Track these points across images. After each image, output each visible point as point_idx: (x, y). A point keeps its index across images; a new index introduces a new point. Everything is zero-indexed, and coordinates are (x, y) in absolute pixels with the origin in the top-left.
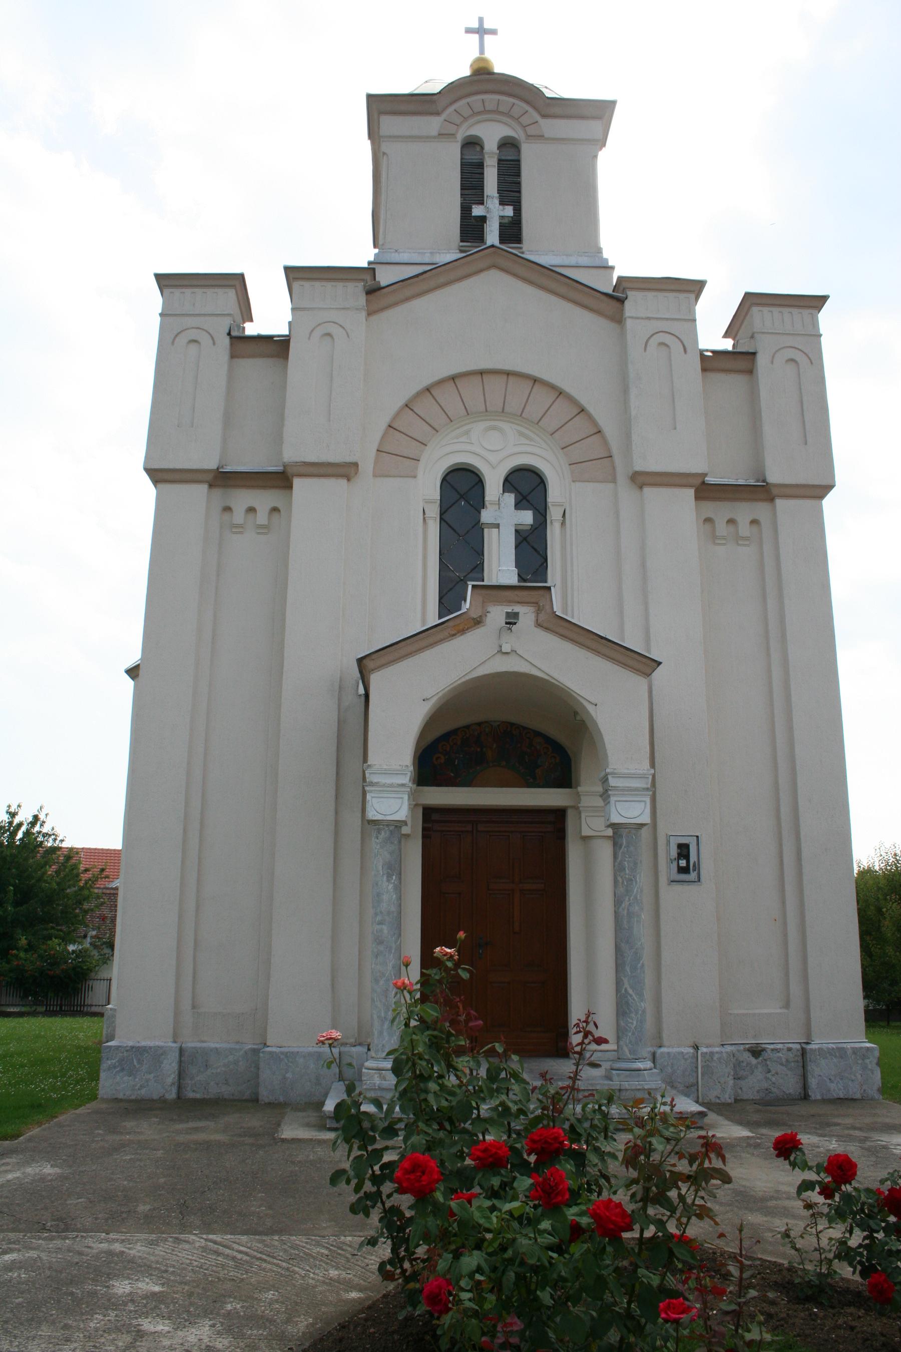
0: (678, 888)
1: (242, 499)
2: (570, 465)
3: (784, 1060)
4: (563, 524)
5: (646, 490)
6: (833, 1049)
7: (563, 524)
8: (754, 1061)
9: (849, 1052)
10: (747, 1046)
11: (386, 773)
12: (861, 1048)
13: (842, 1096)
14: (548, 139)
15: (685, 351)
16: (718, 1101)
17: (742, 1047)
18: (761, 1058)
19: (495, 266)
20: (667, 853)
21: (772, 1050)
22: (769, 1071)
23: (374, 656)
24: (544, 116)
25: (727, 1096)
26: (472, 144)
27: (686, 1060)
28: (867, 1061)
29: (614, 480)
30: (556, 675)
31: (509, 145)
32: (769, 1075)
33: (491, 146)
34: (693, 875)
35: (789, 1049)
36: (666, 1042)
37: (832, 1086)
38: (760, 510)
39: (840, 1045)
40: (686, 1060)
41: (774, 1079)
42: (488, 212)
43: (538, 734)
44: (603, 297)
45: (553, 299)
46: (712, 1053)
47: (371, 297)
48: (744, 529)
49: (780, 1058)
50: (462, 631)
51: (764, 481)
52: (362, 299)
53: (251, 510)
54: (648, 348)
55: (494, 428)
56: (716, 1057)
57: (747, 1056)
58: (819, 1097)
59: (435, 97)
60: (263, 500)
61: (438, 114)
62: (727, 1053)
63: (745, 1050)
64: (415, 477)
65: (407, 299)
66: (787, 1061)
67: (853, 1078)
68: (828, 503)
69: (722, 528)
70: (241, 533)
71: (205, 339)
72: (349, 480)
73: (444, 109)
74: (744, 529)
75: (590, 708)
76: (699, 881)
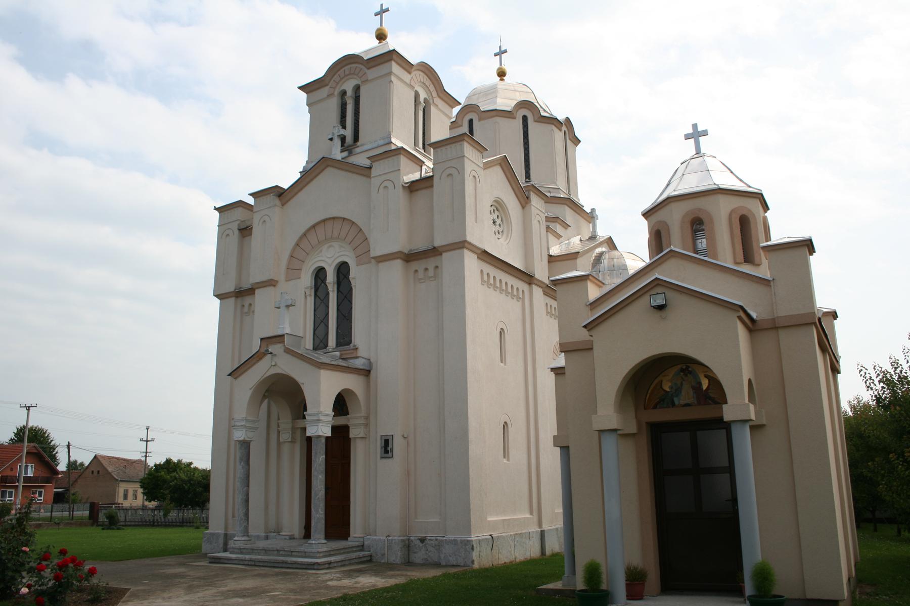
0: (384, 461)
3: (434, 545)
5: (381, 264)
6: (452, 540)
8: (421, 545)
9: (459, 542)
10: (420, 537)
11: (239, 421)
12: (464, 540)
13: (455, 564)
14: (370, 80)
15: (395, 188)
16: (394, 563)
17: (417, 538)
18: (424, 543)
19: (328, 166)
20: (379, 444)
21: (429, 539)
22: (427, 550)
23: (233, 374)
25: (398, 560)
27: (381, 542)
28: (467, 547)
32: (427, 552)
34: (390, 454)
35: (436, 540)
36: (378, 534)
37: (451, 558)
39: (456, 538)
40: (381, 542)
41: (429, 554)
44: (366, 169)
45: (350, 174)
46: (392, 540)
47: (281, 198)
48: (431, 272)
49: (432, 543)
50: (261, 359)
52: (277, 201)
55: (330, 246)
56: (394, 541)
57: (418, 542)
58: (444, 564)
59: (323, 79)
61: (327, 85)
62: (398, 540)
63: (418, 539)
64: (300, 278)
65: (297, 193)
66: (435, 545)
67: (460, 555)
69: (421, 274)
70: (248, 315)
72: (274, 286)
73: (329, 82)
76: (392, 457)
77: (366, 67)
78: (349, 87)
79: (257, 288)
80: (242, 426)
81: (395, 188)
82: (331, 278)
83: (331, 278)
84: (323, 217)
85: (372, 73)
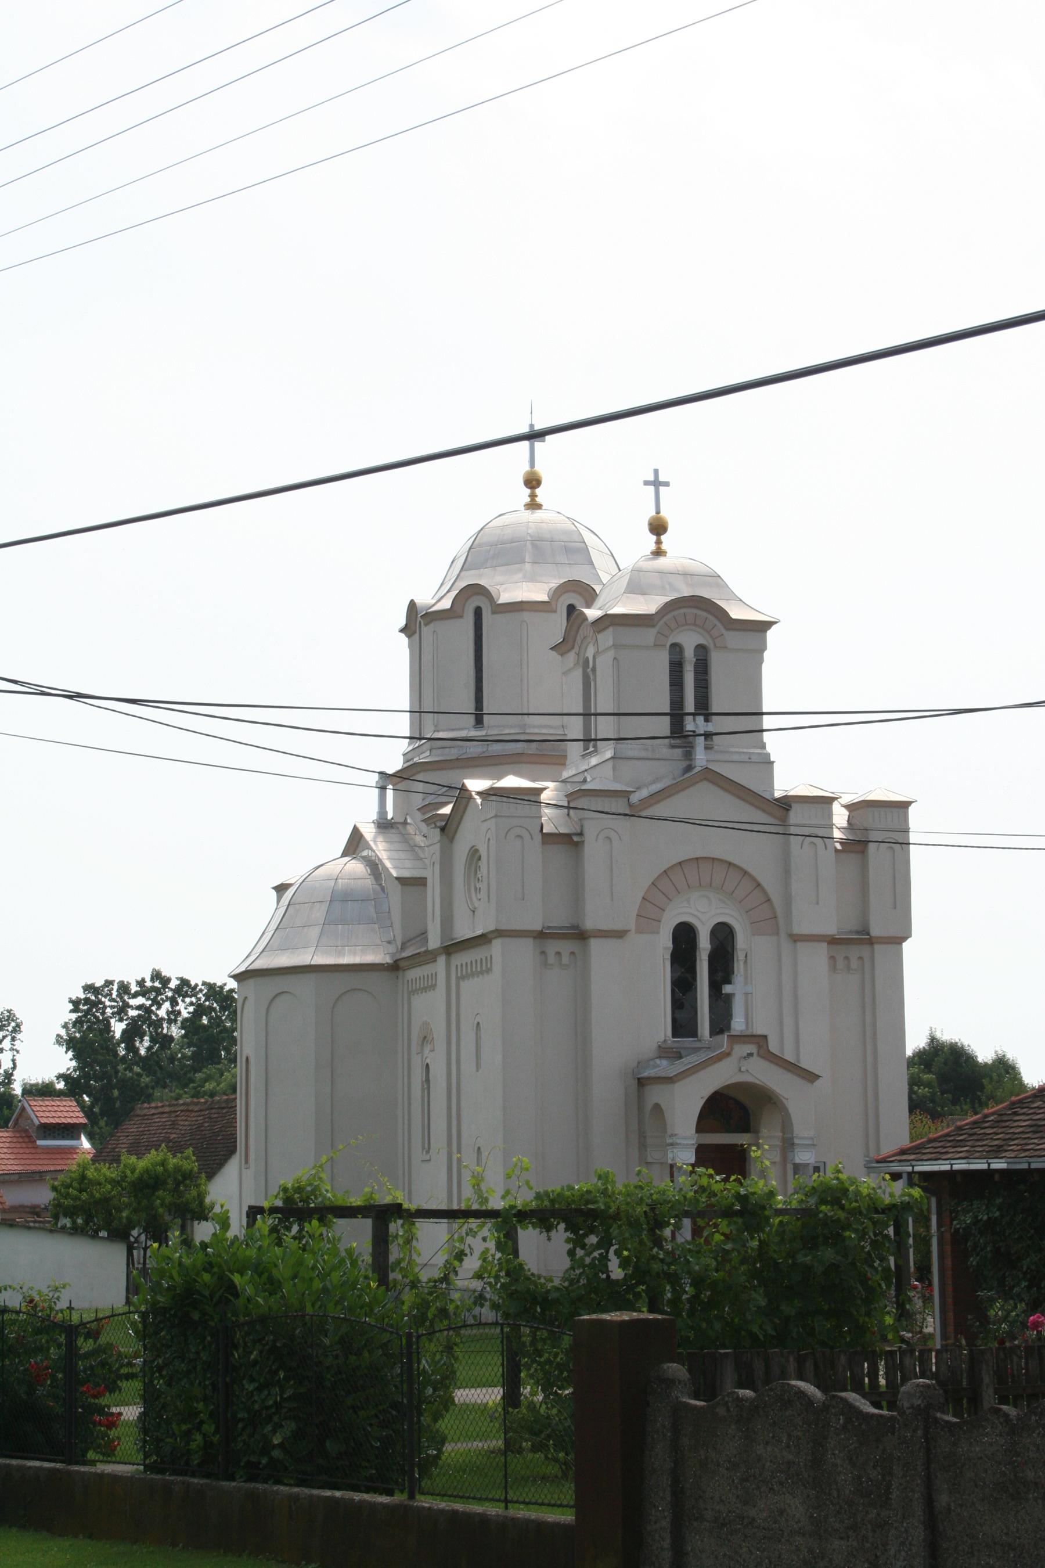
1: (553, 947)
2: (751, 923)
4: (746, 962)
5: (799, 944)
7: (746, 962)
11: (685, 1138)
15: (826, 848)
24: (728, 629)
26: (676, 649)
29: (777, 934)
30: (768, 1084)
31: (702, 652)
33: (689, 654)
38: (865, 951)
42: (697, 727)
43: (731, 1098)
45: (742, 803)
48: (854, 964)
51: (868, 934)
53: (558, 953)
54: (804, 846)
60: (565, 947)
61: (653, 626)
64: (658, 933)
68: (906, 946)
69: (840, 963)
71: (527, 837)
73: (658, 622)
74: (854, 964)
75: (784, 1100)
77: (725, 628)
78: (689, 641)
79: (595, 937)
80: (687, 1144)
81: (826, 848)
82: (704, 944)
83: (704, 944)
84: (698, 855)
85: (733, 639)
